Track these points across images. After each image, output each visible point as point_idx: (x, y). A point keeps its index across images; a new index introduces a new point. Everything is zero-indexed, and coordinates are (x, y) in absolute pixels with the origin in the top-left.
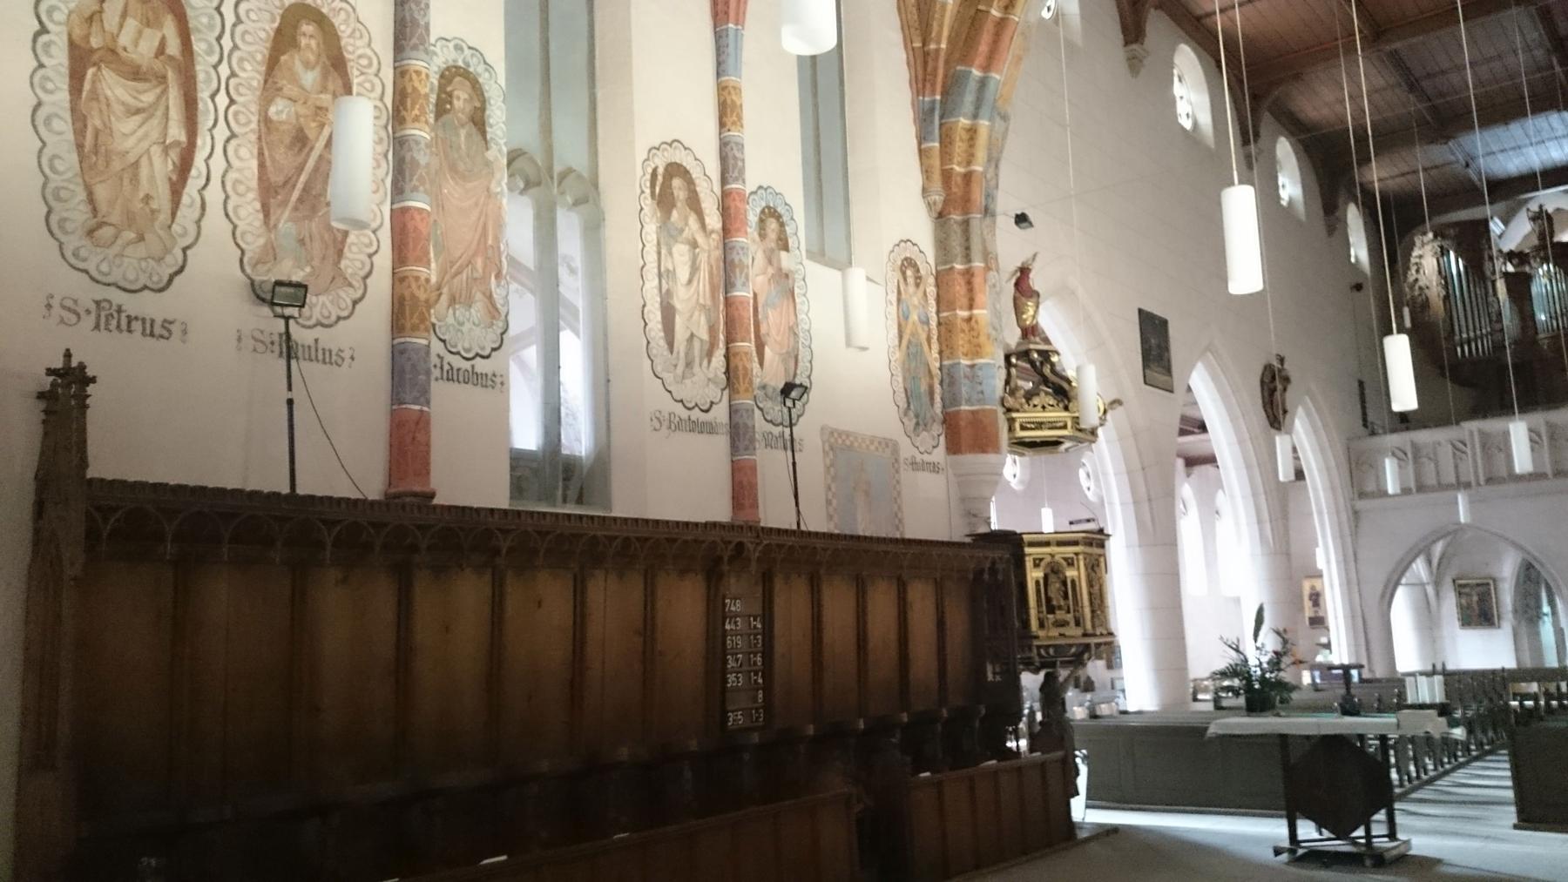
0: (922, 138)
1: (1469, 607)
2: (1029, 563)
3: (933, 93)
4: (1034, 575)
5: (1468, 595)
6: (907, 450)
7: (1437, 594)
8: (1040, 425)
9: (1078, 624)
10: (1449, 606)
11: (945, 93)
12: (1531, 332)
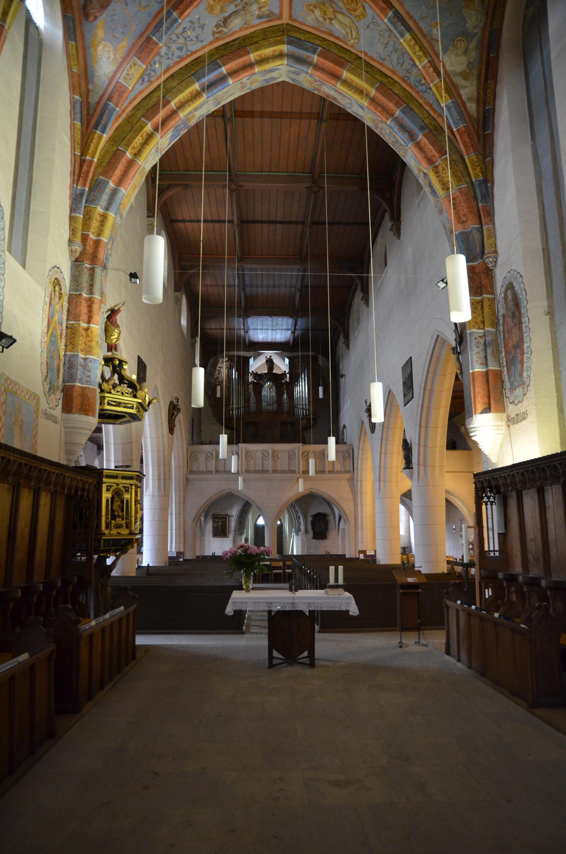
0: (72, 210)
1: (217, 527)
2: (104, 489)
3: (84, 185)
4: (106, 495)
5: (218, 522)
6: (43, 405)
7: (205, 521)
8: (119, 404)
9: (127, 527)
10: (209, 527)
11: (91, 189)
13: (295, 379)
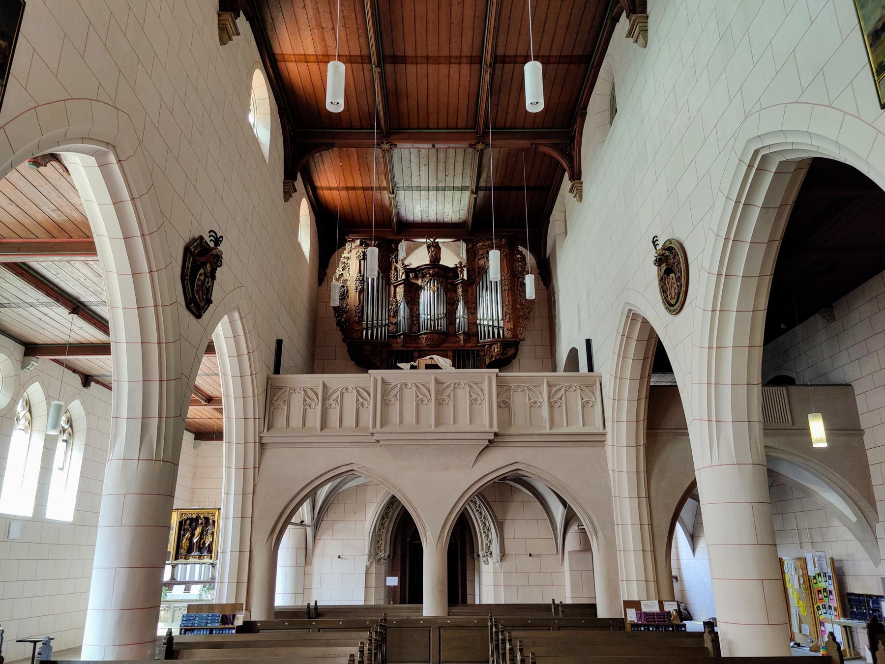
12: (414, 329)
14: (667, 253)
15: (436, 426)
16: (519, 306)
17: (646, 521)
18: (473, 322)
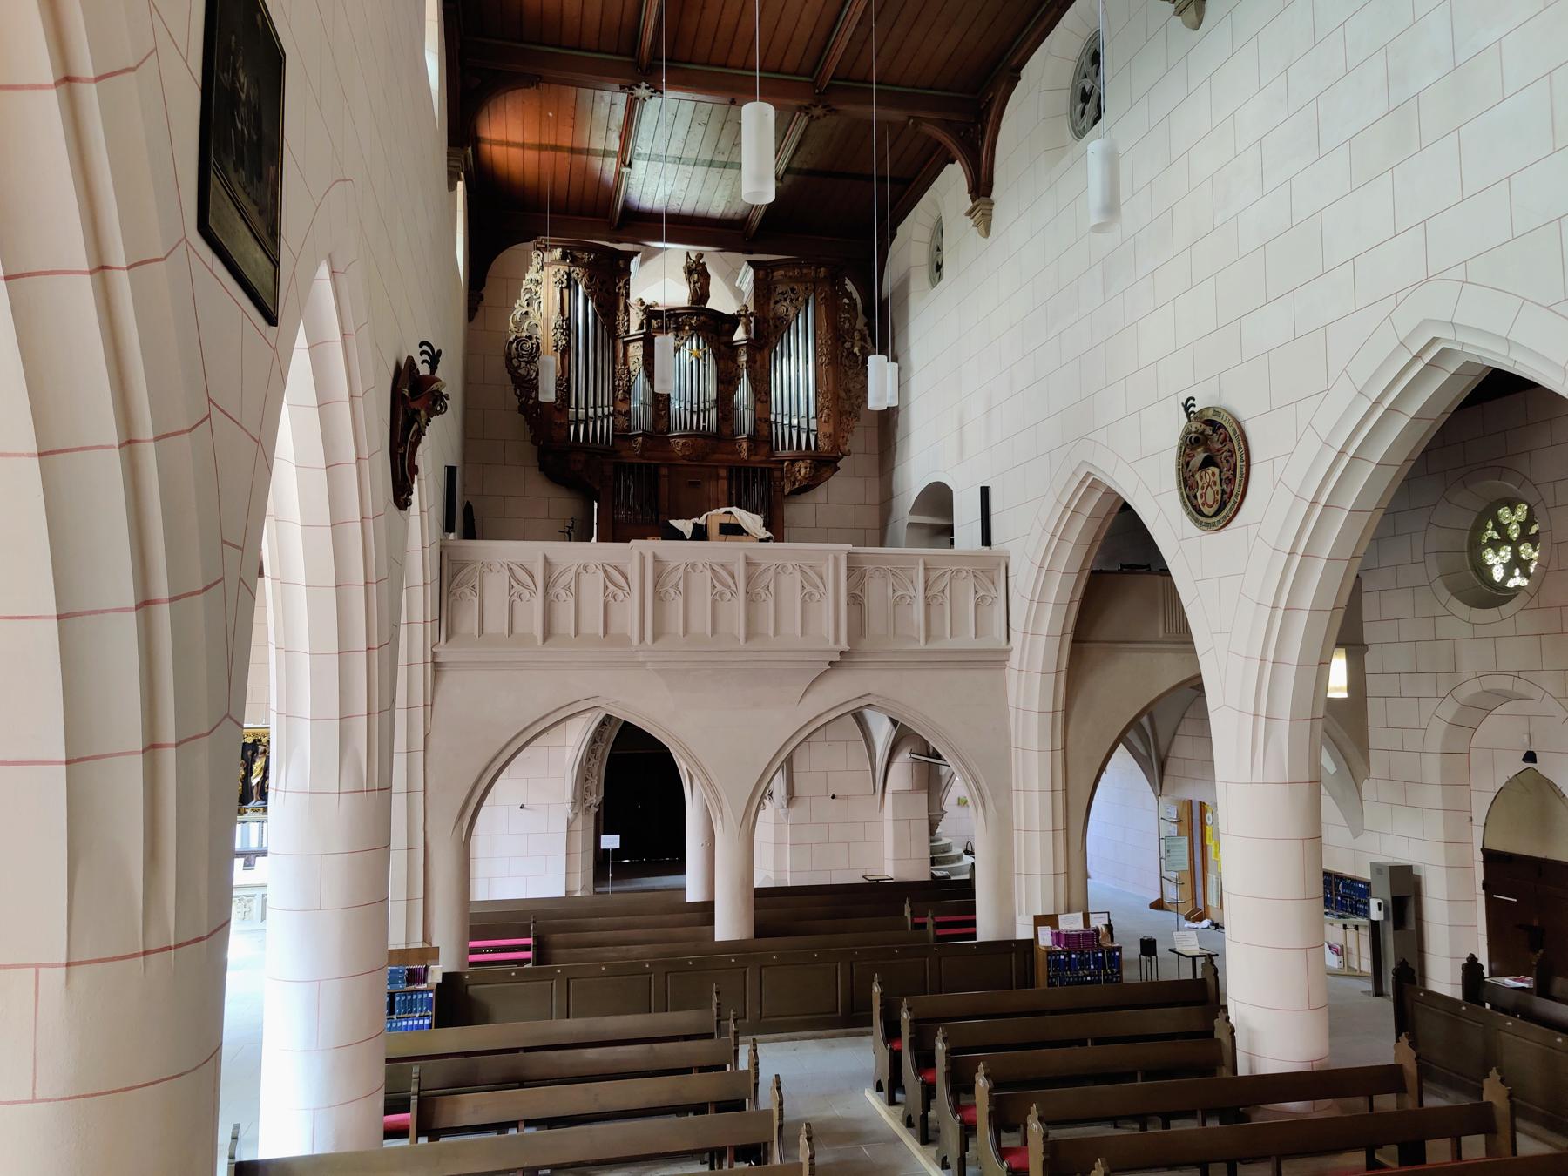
12: (662, 425)
13: (769, 333)
14: (1209, 431)
15: (747, 639)
16: (843, 394)
17: (1060, 786)
18: (763, 419)
